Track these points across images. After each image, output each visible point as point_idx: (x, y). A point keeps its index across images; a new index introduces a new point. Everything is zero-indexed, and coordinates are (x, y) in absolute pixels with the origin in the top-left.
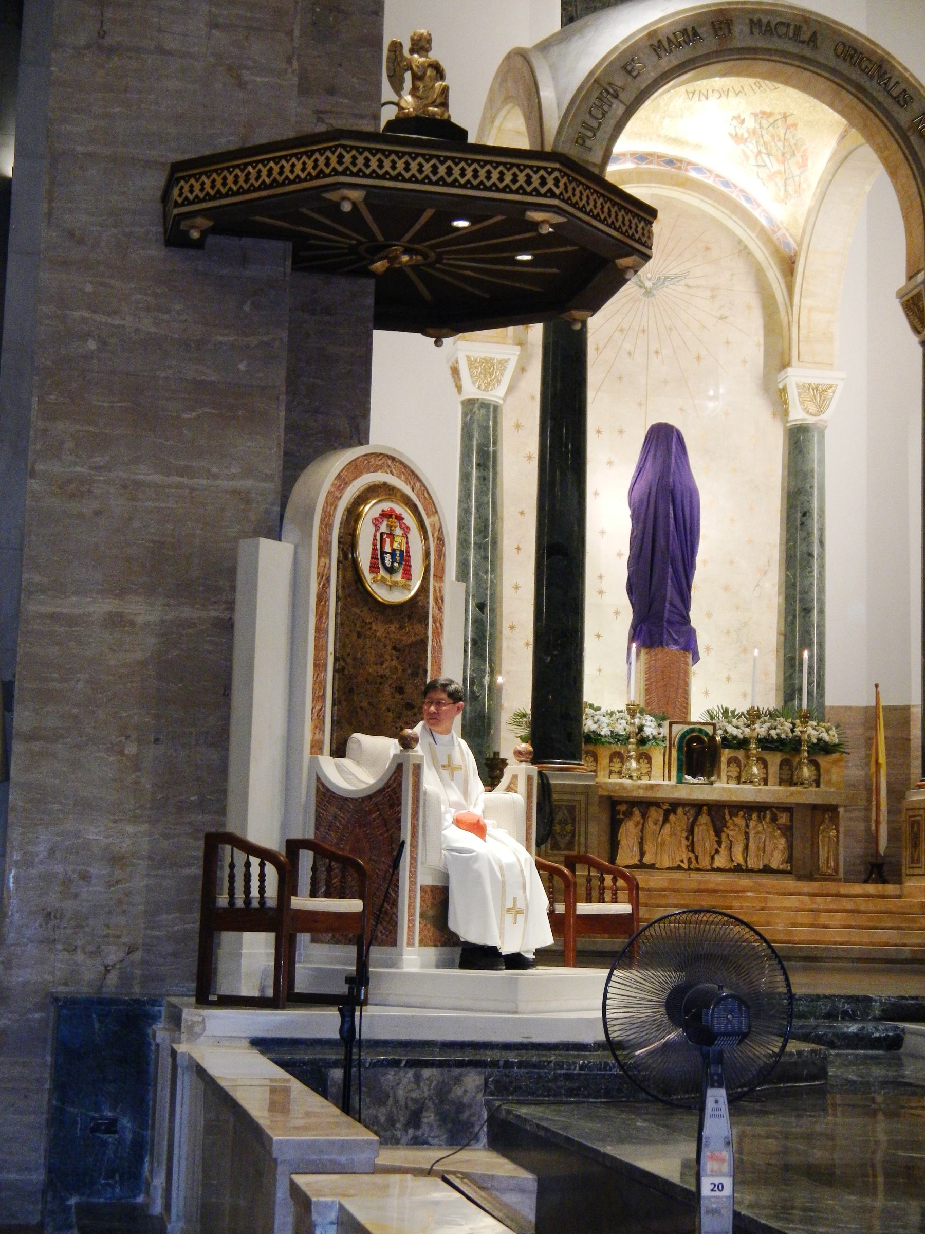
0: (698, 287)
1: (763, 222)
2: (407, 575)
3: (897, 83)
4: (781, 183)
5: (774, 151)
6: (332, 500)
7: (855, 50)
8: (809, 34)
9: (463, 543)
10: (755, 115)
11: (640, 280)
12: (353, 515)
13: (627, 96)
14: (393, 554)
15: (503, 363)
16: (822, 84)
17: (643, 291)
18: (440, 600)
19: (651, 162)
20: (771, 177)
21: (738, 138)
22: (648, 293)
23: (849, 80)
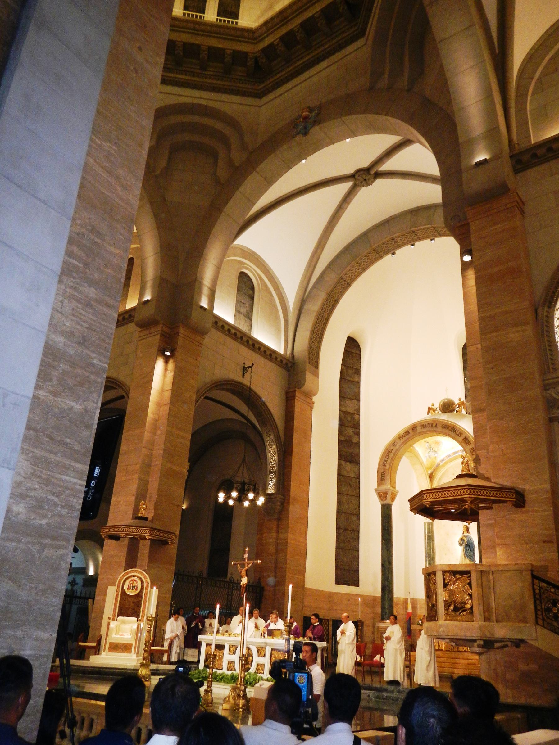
2: (137, 589)
6: (121, 579)
9: (426, 561)
12: (125, 581)
14: (133, 587)
18: (146, 593)
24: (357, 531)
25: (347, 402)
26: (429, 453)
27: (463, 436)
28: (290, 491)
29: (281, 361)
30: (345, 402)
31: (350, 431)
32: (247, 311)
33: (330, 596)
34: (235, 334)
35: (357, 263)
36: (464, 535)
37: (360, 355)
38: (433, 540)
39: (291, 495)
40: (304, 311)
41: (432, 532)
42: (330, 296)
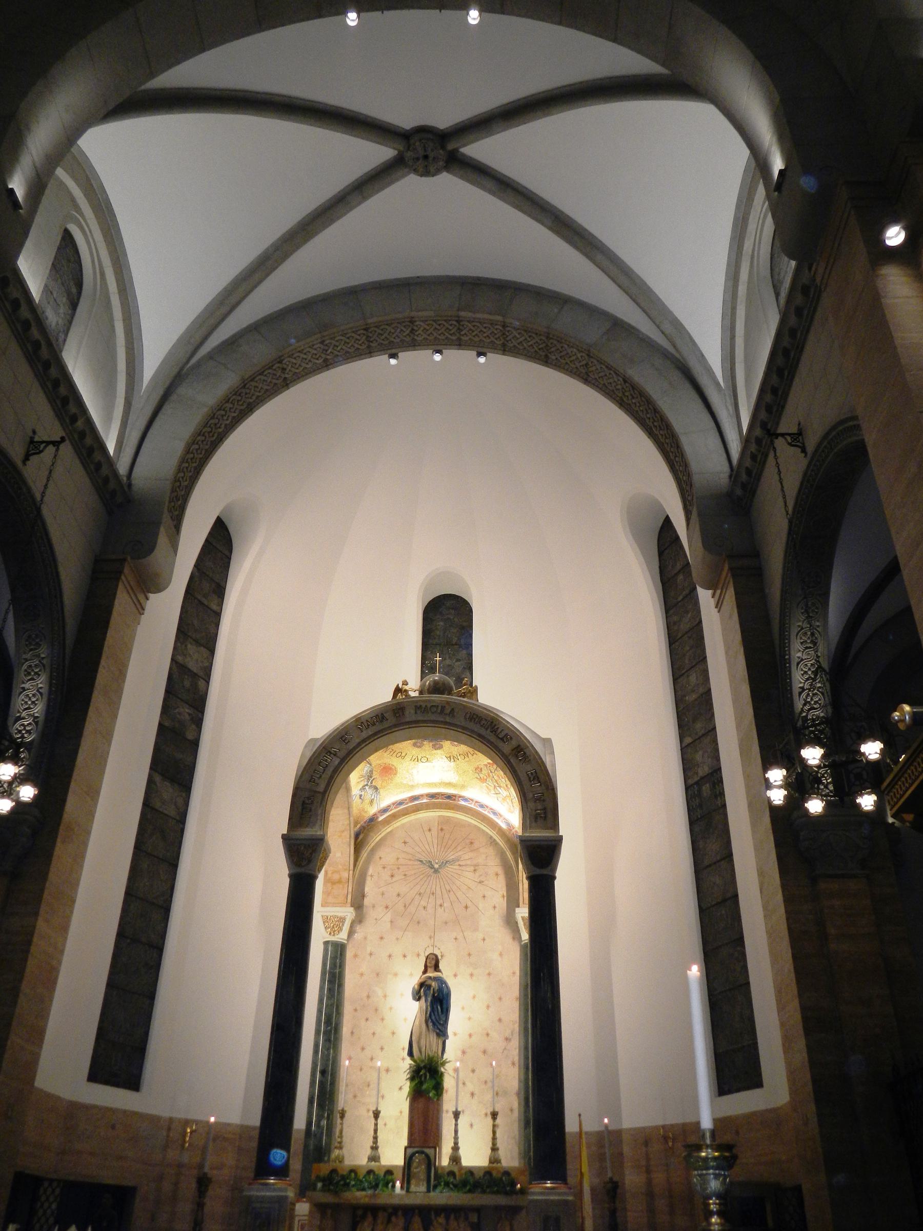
0: (466, 865)
1: (504, 826)
3: (503, 730)
4: (510, 803)
5: (501, 785)
7: (477, 716)
8: (450, 710)
10: (486, 765)
11: (431, 864)
13: (342, 754)
15: (342, 920)
16: (464, 737)
17: (433, 870)
19: (438, 798)
20: (504, 799)
21: (483, 780)
22: (436, 871)
23: (472, 731)
24: (158, 948)
25: (189, 646)
26: (363, 788)
27: (514, 743)
28: (64, 801)
29: (106, 480)
30: (186, 646)
31: (185, 711)
32: (57, 324)
33: (74, 1110)
34: (37, 345)
35: (322, 342)
36: (429, 974)
37: (230, 559)
38: (341, 986)
39: (65, 816)
40: (174, 397)
41: (342, 966)
42: (244, 387)
